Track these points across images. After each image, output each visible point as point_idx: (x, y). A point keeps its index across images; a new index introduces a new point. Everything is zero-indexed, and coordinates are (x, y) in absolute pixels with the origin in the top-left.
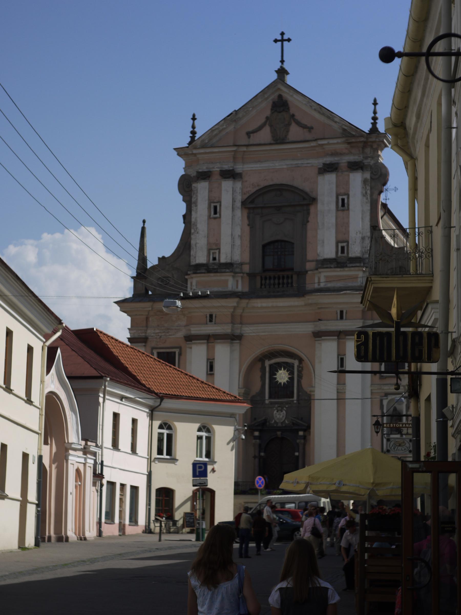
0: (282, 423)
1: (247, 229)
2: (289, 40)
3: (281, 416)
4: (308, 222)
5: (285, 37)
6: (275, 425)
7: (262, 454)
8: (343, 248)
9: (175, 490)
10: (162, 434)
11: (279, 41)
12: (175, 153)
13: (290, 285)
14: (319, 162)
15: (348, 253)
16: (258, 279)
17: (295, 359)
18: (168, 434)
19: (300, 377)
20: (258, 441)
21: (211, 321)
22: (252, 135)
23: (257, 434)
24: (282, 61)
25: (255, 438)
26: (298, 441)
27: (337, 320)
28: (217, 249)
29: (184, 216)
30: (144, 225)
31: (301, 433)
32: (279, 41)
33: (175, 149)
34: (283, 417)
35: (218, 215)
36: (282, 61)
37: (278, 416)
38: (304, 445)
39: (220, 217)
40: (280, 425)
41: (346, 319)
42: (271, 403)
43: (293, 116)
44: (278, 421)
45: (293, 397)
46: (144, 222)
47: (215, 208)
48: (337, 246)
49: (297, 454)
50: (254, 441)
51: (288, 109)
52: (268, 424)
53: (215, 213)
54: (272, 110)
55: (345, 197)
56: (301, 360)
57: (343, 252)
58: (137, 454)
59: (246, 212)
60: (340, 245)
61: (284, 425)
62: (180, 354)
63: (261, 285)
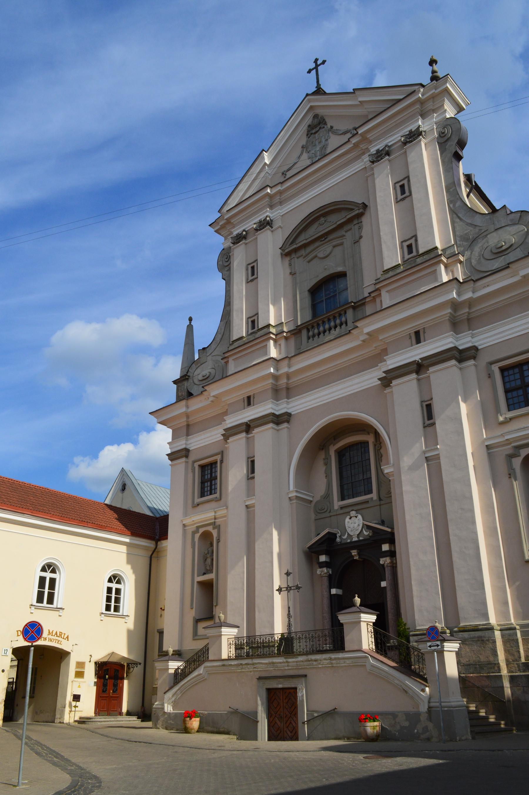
1: (289, 278)
2: (324, 62)
3: (356, 525)
4: (361, 237)
5: (319, 62)
6: (349, 541)
7: (334, 591)
8: (410, 247)
11: (313, 69)
12: (211, 230)
13: (344, 326)
15: (417, 251)
16: (304, 332)
17: (369, 434)
19: (379, 458)
20: (325, 570)
21: (249, 404)
22: (287, 173)
23: (323, 558)
26: (382, 562)
27: (412, 346)
30: (190, 323)
31: (385, 547)
32: (313, 69)
33: (210, 225)
34: (359, 525)
35: (255, 276)
37: (352, 526)
38: (394, 567)
39: (257, 278)
40: (355, 539)
41: (425, 341)
42: (342, 508)
43: (332, 127)
44: (352, 534)
45: (370, 492)
46: (190, 319)
47: (253, 268)
49: (383, 584)
50: (319, 571)
51: (325, 124)
52: (338, 540)
53: (253, 274)
54: (307, 135)
55: (405, 182)
57: (410, 251)
59: (287, 260)
61: (361, 538)
62: (222, 461)
63: (309, 338)
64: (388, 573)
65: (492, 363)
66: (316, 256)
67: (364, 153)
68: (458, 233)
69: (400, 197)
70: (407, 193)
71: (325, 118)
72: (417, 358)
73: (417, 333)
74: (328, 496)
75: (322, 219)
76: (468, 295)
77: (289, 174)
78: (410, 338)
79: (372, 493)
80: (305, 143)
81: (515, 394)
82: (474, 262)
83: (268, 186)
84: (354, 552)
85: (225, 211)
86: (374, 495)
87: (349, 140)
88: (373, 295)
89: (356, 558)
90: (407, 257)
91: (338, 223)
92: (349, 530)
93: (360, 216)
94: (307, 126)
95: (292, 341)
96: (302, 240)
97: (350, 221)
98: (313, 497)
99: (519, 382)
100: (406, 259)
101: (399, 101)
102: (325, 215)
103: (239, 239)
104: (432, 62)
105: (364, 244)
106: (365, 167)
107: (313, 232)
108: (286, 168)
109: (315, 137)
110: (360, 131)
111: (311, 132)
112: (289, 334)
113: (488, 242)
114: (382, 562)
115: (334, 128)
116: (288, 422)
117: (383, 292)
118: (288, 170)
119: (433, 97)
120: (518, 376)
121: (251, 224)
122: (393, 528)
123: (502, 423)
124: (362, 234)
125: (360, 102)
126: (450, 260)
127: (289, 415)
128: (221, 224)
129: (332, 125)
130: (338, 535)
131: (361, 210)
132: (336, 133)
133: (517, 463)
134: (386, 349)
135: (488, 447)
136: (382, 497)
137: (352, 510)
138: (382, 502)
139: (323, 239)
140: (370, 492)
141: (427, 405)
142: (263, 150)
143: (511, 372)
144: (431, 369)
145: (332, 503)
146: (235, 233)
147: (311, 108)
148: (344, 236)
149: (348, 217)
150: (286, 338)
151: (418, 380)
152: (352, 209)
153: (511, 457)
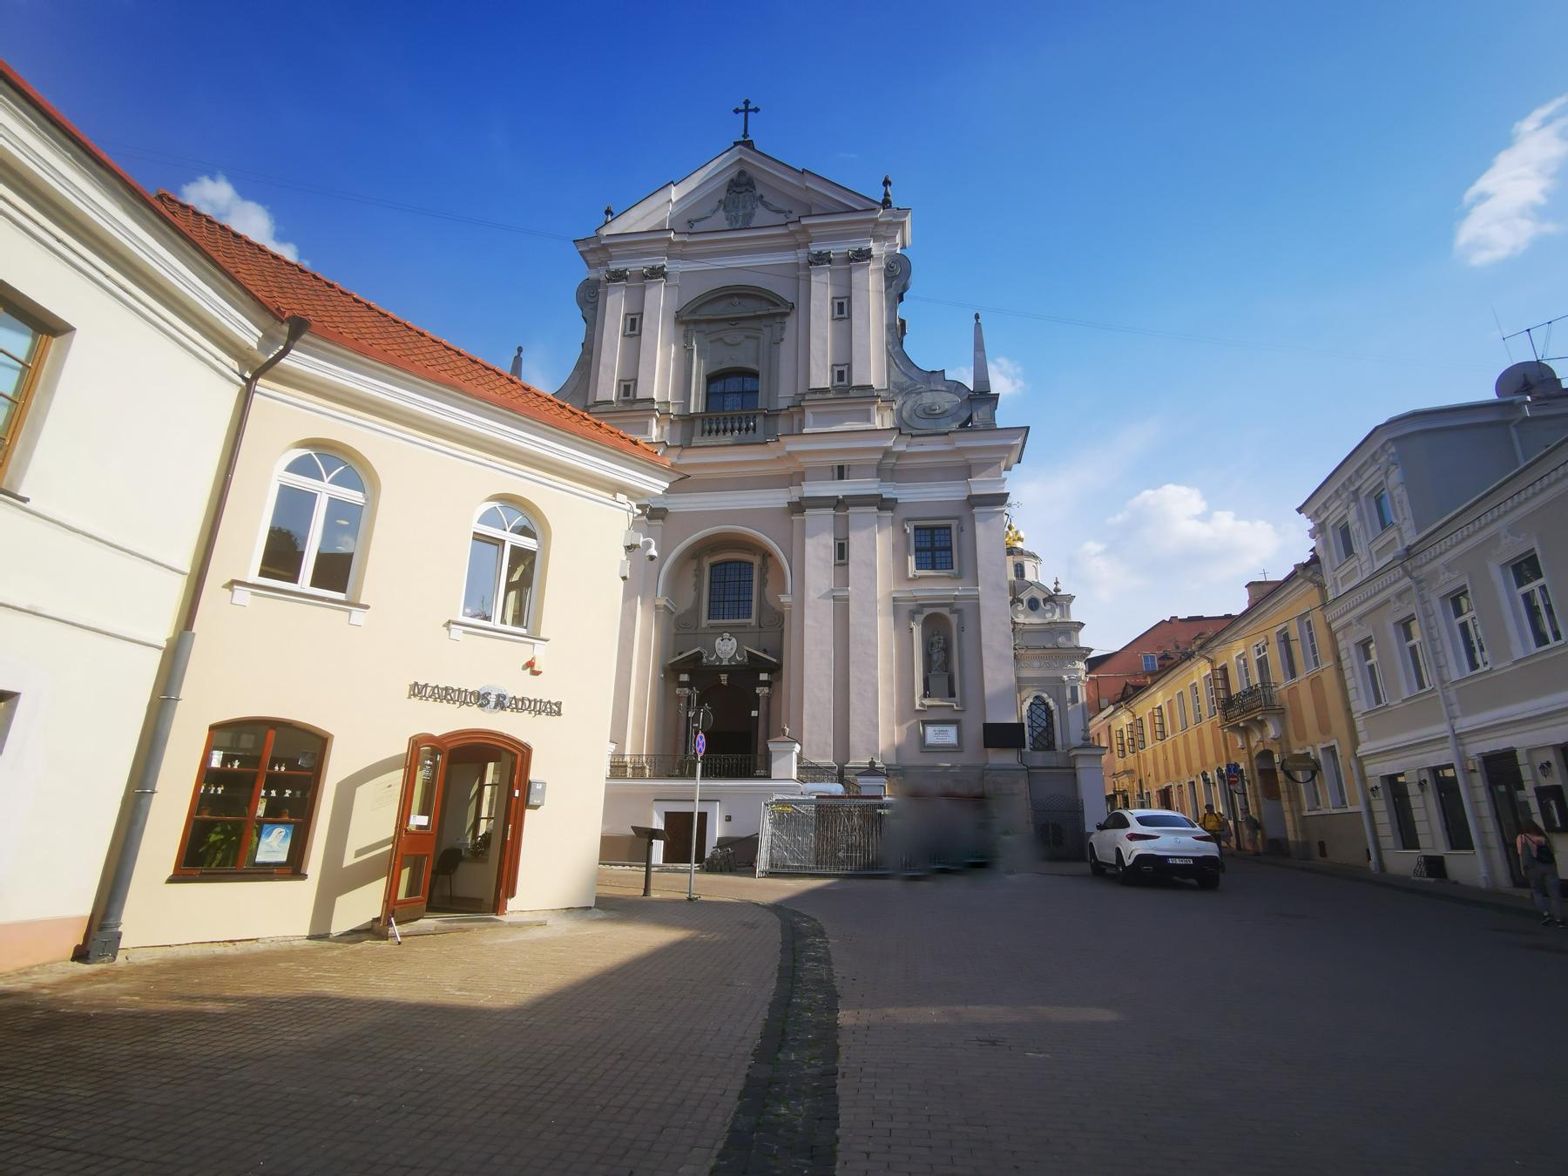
0: (730, 659)
2: (756, 110)
4: (782, 340)
6: (718, 663)
8: (841, 374)
9: (333, 736)
10: (311, 498)
11: (741, 111)
13: (751, 432)
14: (802, 256)
15: (850, 381)
16: (698, 425)
17: (755, 555)
18: (335, 506)
19: (763, 582)
20: (687, 690)
23: (684, 678)
24: (745, 135)
25: (682, 685)
27: (833, 480)
28: (631, 380)
29: (583, 344)
30: (519, 355)
31: (764, 677)
32: (741, 111)
34: (732, 649)
35: (636, 332)
36: (745, 135)
38: (768, 698)
39: (640, 334)
40: (725, 663)
41: (848, 479)
42: (712, 627)
43: (762, 197)
45: (749, 616)
48: (832, 371)
50: (678, 691)
51: (754, 188)
52: (705, 660)
54: (728, 191)
55: (845, 301)
56: (766, 555)
58: (25, 500)
59: (683, 328)
60: (837, 369)
61: (733, 663)
64: (762, 704)
65: (909, 520)
66: (721, 339)
67: (798, 246)
68: (892, 379)
69: (836, 315)
70: (845, 315)
71: (755, 182)
72: (840, 495)
73: (841, 468)
74: (696, 609)
75: (736, 299)
76: (901, 448)
77: (698, 227)
78: (833, 470)
79: (750, 618)
80: (723, 199)
81: (923, 554)
82: (904, 414)
83: (673, 229)
84: (724, 677)
85: (605, 234)
86: (753, 621)
87: (786, 224)
88: (791, 410)
89: (725, 683)
90: (836, 383)
91: (758, 313)
92: (719, 652)
93: (786, 315)
94: (728, 179)
95: (679, 428)
96: (707, 313)
97: (773, 316)
98: (675, 609)
99: (929, 545)
100: (834, 385)
101: (855, 211)
102: (738, 295)
103: (618, 276)
104: (887, 183)
105: (786, 350)
106: (798, 263)
107: (720, 310)
108: (694, 218)
109: (739, 198)
110: (804, 222)
111: (735, 189)
112: (676, 419)
113: (922, 400)
114: (757, 692)
115: (764, 199)
116: (663, 519)
117: (808, 413)
118: (697, 221)
119: (889, 224)
120: (929, 538)
121: (642, 264)
122: (780, 657)
123: (911, 579)
124: (783, 337)
125: (806, 187)
126: (884, 404)
127: (665, 510)
128: (591, 246)
129: (763, 194)
130: (705, 656)
131: (788, 310)
132: (766, 205)
133: (920, 618)
134: (803, 474)
135: (894, 599)
136: (762, 625)
137: (725, 632)
138: (762, 630)
139: (734, 323)
140: (750, 618)
141: (839, 544)
142: (672, 182)
143: (923, 532)
144: (851, 510)
145: (698, 621)
146: (613, 267)
147: (741, 159)
148: (761, 330)
149: (771, 311)
150: (671, 421)
151: (835, 516)
152: (778, 305)
153: (913, 614)
